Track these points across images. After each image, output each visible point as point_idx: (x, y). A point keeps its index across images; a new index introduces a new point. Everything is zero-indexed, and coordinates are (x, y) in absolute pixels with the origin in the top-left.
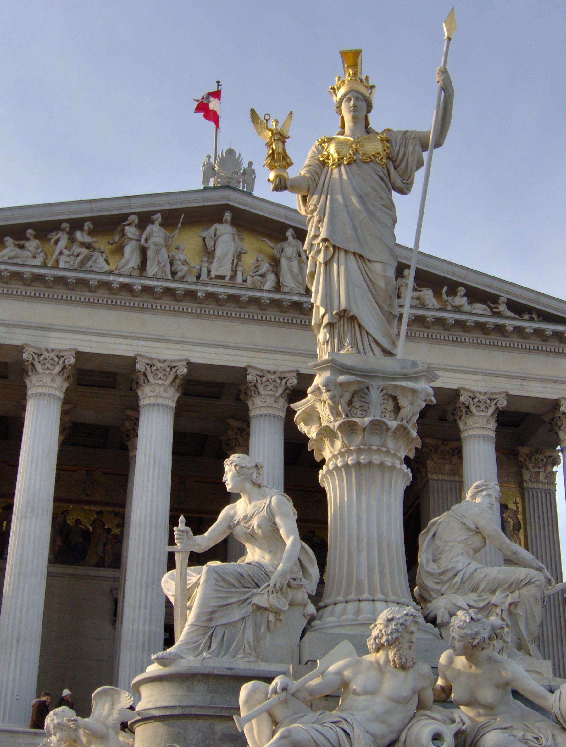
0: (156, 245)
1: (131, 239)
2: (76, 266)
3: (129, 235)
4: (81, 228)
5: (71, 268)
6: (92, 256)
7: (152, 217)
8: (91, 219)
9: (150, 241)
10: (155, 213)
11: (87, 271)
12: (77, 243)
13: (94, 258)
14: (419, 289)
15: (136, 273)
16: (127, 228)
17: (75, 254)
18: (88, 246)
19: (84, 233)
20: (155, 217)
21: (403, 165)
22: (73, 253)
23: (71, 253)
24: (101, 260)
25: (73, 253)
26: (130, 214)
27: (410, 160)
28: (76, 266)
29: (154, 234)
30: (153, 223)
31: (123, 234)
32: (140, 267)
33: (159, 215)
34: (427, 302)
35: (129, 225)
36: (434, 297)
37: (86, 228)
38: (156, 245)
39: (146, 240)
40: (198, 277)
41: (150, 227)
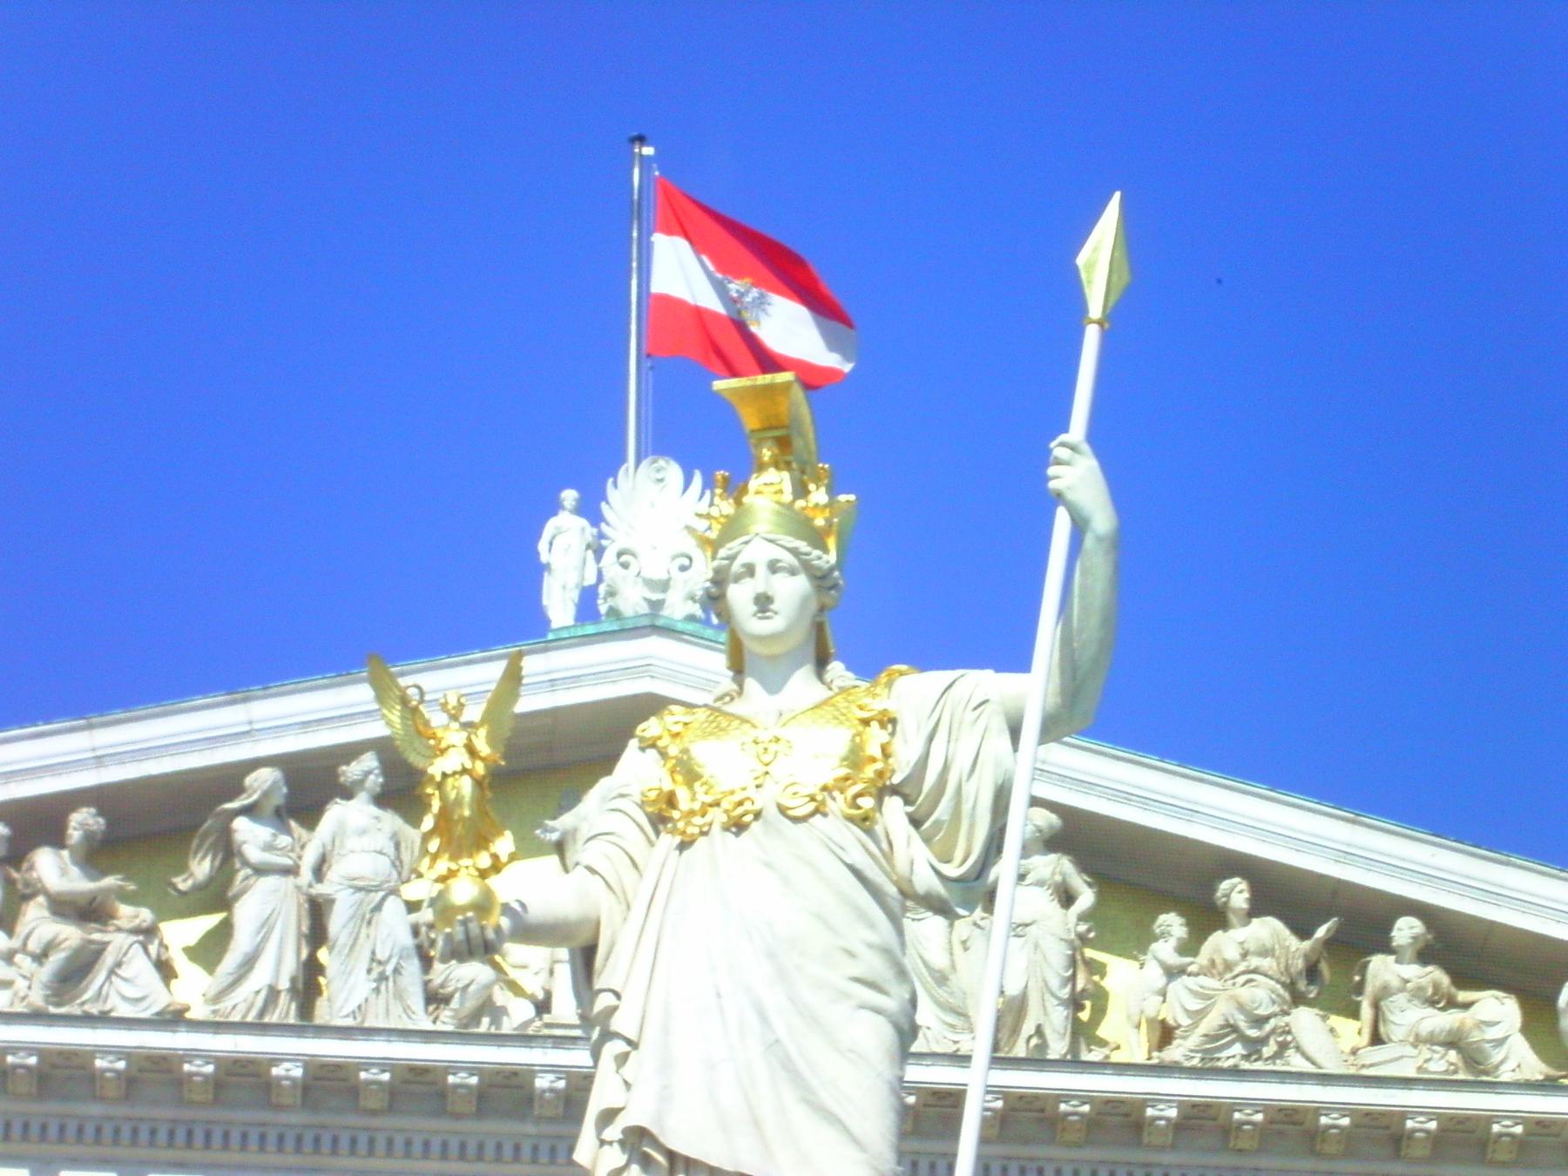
0: (359, 889)
1: (261, 871)
2: (37, 998)
3: (253, 853)
4: (56, 839)
5: (19, 1008)
6: (101, 948)
7: (344, 768)
8: (95, 796)
9: (334, 874)
10: (350, 752)
11: (88, 1020)
12: (41, 899)
13: (109, 959)
14: (1463, 996)
15: (285, 1010)
16: (241, 825)
17: (34, 945)
18: (89, 912)
19: (65, 853)
20: (351, 771)
21: (942, 811)
22: (25, 944)
23: (15, 943)
24: (139, 967)
25: (25, 944)
26: (255, 764)
27: (969, 790)
28: (37, 998)
29: (352, 843)
30: (347, 793)
31: (228, 851)
32: (300, 986)
33: (369, 761)
34: (1496, 1056)
35: (248, 811)
36: (1526, 1030)
37: (74, 835)
38: (359, 889)
39: (319, 873)
40: (543, 1007)
41: (337, 813)
